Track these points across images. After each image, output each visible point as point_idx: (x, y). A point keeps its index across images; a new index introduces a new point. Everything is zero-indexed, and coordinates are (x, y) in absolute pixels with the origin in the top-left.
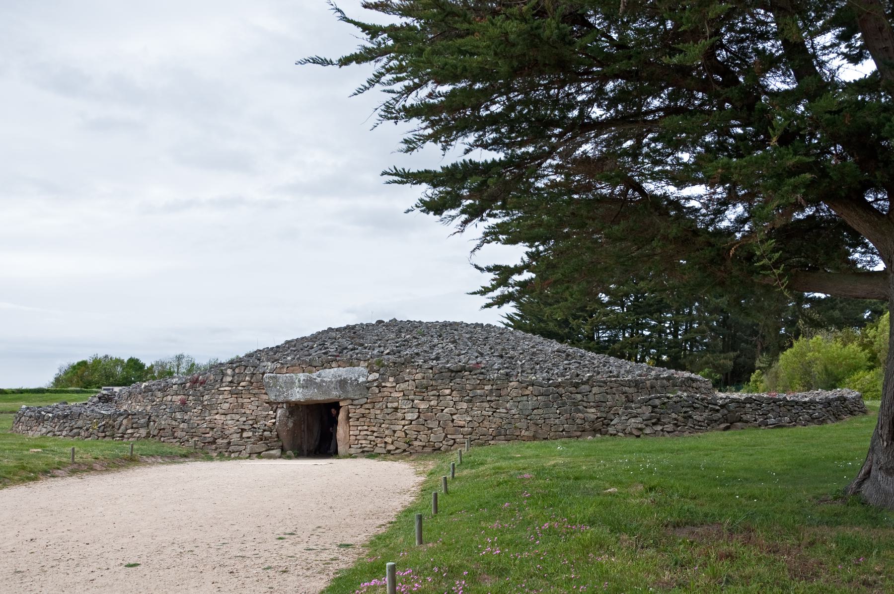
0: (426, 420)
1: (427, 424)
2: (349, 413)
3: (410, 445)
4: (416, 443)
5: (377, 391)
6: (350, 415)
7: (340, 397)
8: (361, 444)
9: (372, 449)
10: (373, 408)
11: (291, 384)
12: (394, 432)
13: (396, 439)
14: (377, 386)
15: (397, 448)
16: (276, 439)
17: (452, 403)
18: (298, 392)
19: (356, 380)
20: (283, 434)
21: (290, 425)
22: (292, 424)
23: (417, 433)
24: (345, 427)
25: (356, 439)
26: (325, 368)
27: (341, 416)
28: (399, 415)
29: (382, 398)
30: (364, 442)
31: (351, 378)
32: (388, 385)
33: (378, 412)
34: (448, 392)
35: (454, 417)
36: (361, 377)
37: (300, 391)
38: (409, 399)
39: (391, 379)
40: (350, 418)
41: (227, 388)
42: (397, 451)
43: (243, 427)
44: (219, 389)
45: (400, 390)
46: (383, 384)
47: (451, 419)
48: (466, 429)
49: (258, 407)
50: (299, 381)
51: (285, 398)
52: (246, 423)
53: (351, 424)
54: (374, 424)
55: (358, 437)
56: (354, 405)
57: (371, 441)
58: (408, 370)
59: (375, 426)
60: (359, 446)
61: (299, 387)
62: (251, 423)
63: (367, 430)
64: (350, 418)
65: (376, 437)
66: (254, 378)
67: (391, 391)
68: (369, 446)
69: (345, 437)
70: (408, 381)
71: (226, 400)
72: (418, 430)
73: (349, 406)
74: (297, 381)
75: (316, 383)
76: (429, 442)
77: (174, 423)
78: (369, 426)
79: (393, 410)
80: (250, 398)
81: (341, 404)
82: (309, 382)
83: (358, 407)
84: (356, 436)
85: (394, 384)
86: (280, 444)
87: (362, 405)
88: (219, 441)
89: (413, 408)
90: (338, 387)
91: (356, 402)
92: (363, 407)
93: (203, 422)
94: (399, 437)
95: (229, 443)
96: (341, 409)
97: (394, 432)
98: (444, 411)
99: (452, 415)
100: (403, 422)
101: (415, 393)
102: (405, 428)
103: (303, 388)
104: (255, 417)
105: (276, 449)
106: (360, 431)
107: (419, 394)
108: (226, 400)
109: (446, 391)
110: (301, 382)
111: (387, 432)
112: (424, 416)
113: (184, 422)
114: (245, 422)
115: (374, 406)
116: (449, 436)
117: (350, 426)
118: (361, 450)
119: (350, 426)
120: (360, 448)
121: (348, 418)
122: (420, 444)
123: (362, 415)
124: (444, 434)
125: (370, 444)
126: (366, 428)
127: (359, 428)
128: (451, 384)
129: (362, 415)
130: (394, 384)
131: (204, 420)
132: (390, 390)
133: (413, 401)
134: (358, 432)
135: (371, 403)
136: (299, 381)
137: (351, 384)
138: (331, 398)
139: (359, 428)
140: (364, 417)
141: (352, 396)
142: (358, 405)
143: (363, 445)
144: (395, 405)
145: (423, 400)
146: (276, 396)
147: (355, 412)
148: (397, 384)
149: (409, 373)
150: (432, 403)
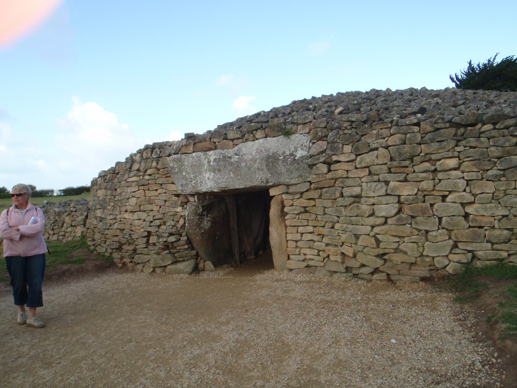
0: (413, 217)
1: (416, 223)
2: (283, 207)
3: (385, 260)
4: (397, 258)
5: (325, 170)
6: (286, 210)
7: (267, 182)
8: (305, 254)
9: (322, 264)
10: (320, 197)
11: (197, 168)
12: (357, 237)
13: (360, 249)
14: (324, 163)
15: (363, 266)
16: (186, 247)
17: (462, 183)
18: (208, 178)
19: (291, 155)
20: (197, 240)
21: (206, 224)
22: (210, 224)
23: (397, 239)
24: (280, 228)
25: (297, 247)
26: (247, 140)
27: (274, 211)
28: (365, 208)
29: (333, 181)
30: (308, 251)
31: (284, 152)
32: (342, 158)
33: (328, 203)
34: (453, 163)
35: (470, 209)
36: (299, 149)
37: (211, 177)
38: (379, 181)
39: (348, 149)
40: (287, 214)
41: (134, 179)
42: (363, 270)
43: (149, 229)
44: (128, 180)
45: (364, 165)
46: (335, 158)
47: (463, 213)
48: (497, 232)
49: (166, 201)
50: (209, 162)
51: (193, 187)
52: (152, 224)
53: (288, 223)
56: (291, 194)
57: (319, 251)
58: (375, 132)
59: (324, 226)
60: (302, 257)
61: (210, 171)
62: (158, 224)
64: (287, 214)
65: (327, 245)
66: (160, 163)
67: (347, 168)
68: (317, 258)
69: (281, 243)
70: (377, 149)
71: (134, 194)
72: (400, 234)
73: (284, 196)
74: (206, 162)
75: (232, 164)
76: (422, 255)
79: (352, 199)
80: (157, 190)
81: (272, 192)
82: (221, 163)
83: (298, 196)
84: (297, 241)
85: (353, 157)
86: (194, 252)
87: (302, 193)
88: (125, 247)
89: (387, 195)
90: (264, 167)
91: (292, 189)
92: (305, 195)
94: (365, 247)
95: (135, 250)
96: (272, 201)
97: (357, 237)
98: (448, 199)
99: (463, 205)
100: (372, 220)
101: (389, 169)
102: (376, 230)
103: (214, 172)
104: (161, 216)
105: (187, 260)
106: (302, 234)
107: (398, 170)
108: (134, 194)
109: (448, 161)
110: (212, 164)
111: (344, 237)
112: (411, 209)
114: (151, 222)
115: (321, 195)
116: (460, 245)
117: (286, 227)
118: (305, 264)
119: (286, 227)
120: (303, 261)
121: (283, 214)
122: (405, 258)
123: (303, 210)
124: (451, 242)
125: (319, 255)
126: (310, 229)
127: (301, 229)
128: (458, 149)
129: (303, 210)
130: (353, 157)
131: (116, 219)
132: (346, 167)
133: (387, 183)
134: (298, 237)
135: (316, 189)
136: (209, 162)
137: (285, 160)
138: (254, 184)
139: (301, 229)
140: (306, 212)
141: (287, 181)
142: (296, 193)
143: (308, 257)
144: (356, 190)
145: (406, 180)
146: (182, 185)
147: (292, 205)
148: (357, 155)
149: (379, 136)
150: (424, 185)
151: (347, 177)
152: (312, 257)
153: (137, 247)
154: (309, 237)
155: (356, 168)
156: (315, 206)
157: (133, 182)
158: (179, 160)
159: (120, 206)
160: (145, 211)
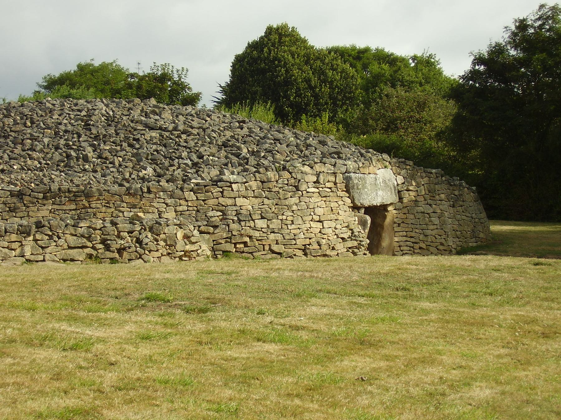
13: (429, 244)
30: (405, 248)
33: (412, 216)
54: (411, 230)
55: (402, 244)
57: (410, 247)
63: (406, 236)
65: (413, 243)
77: (257, 234)
78: (406, 232)
85: (417, 189)
93: (298, 231)
97: (426, 236)
113: (274, 232)
125: (409, 250)
126: (405, 233)
151: (416, 201)
152: (407, 252)
153: (339, 252)
154: (405, 239)
155: (418, 195)
156: (406, 218)
157: (313, 193)
158: (364, 179)
159: (302, 215)
160: (331, 220)
